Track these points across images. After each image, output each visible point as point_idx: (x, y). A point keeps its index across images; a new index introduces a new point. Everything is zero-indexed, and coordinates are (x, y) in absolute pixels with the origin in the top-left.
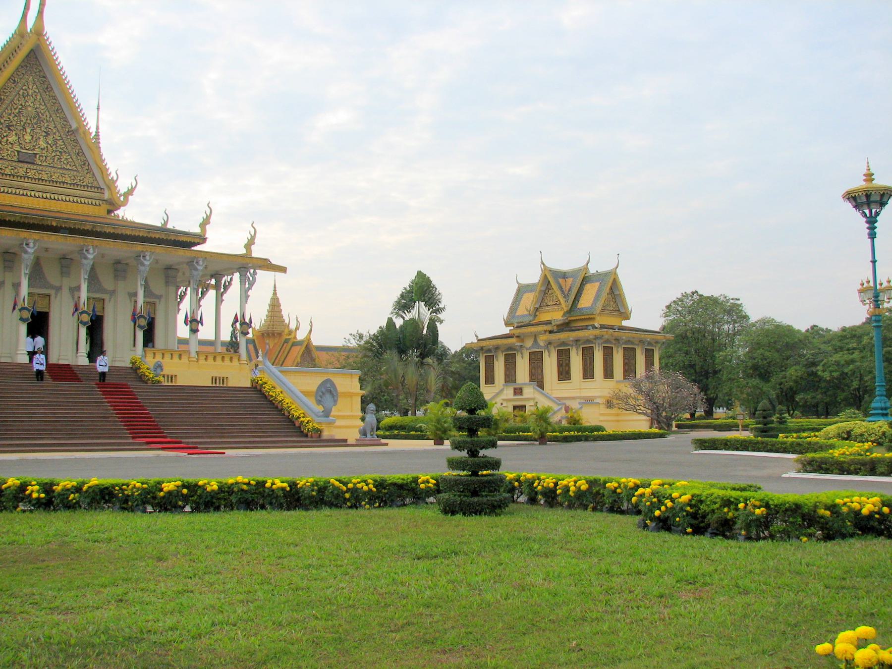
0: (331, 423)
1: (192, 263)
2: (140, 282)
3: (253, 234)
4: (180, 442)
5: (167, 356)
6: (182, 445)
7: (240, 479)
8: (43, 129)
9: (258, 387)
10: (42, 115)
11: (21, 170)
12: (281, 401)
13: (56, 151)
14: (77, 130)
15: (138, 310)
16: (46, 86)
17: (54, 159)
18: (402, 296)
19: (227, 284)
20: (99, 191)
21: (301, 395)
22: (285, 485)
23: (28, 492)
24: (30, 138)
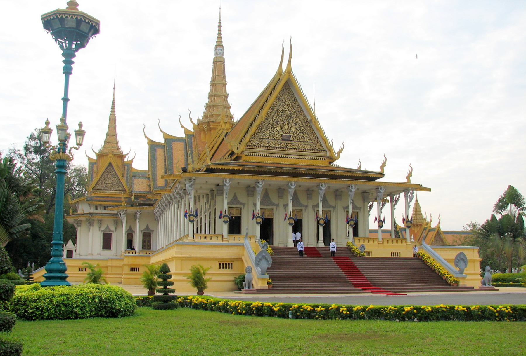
0: (464, 278)
1: (377, 189)
2: (350, 201)
3: (410, 170)
4: (380, 289)
5: (366, 241)
6: (381, 290)
7: (442, 305)
8: (293, 122)
9: (420, 258)
10: (293, 114)
11: (284, 144)
12: (434, 265)
13: (301, 133)
14: (311, 120)
15: (350, 216)
16: (294, 99)
17: (300, 137)
18: (500, 201)
19: (397, 199)
20: (324, 152)
21: (445, 262)
22: (464, 308)
23: (341, 311)
24: (288, 127)
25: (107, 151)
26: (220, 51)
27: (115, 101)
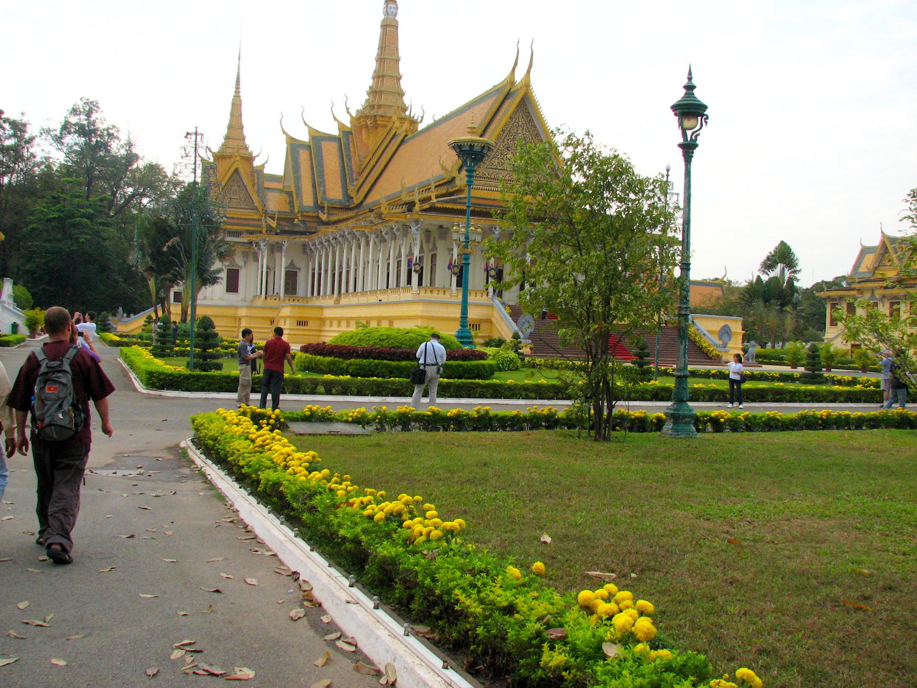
0: (727, 352)
18: (768, 258)
25: (231, 150)
26: (392, 10)
27: (241, 77)
